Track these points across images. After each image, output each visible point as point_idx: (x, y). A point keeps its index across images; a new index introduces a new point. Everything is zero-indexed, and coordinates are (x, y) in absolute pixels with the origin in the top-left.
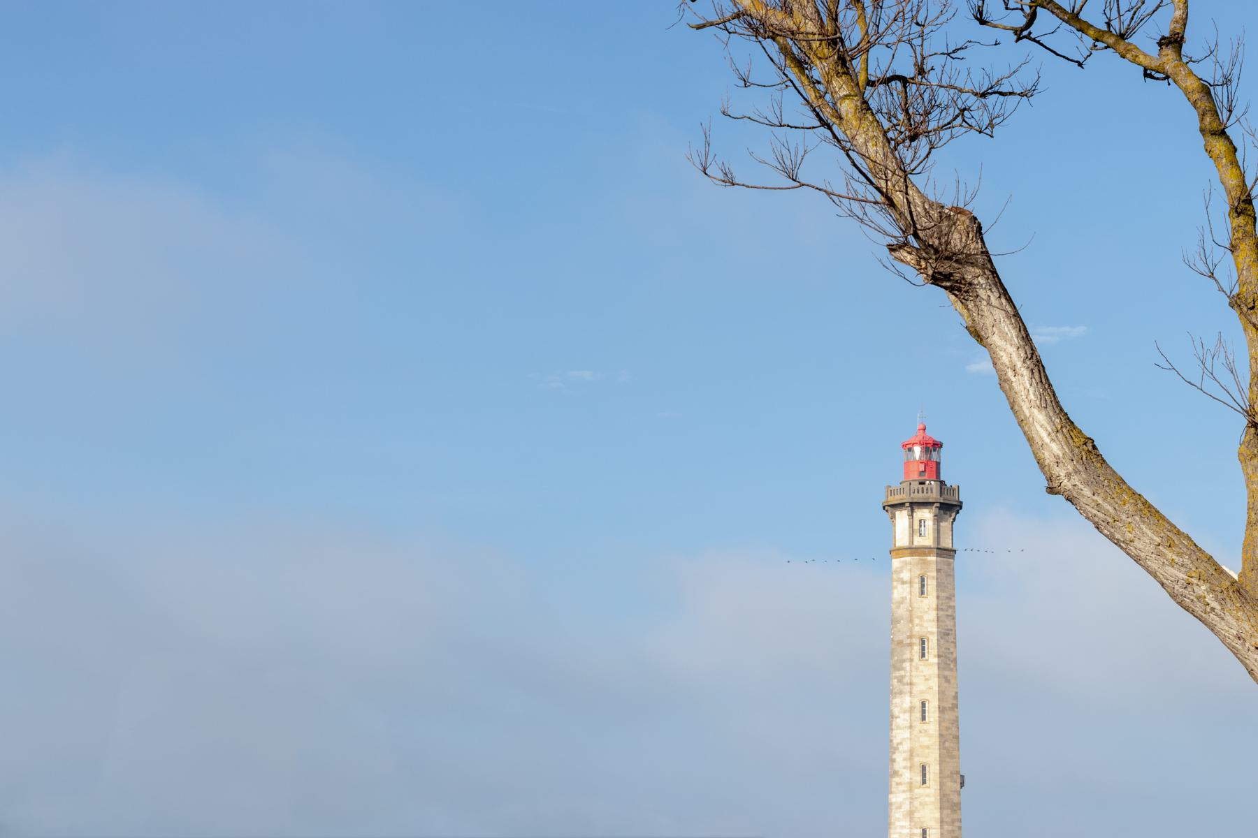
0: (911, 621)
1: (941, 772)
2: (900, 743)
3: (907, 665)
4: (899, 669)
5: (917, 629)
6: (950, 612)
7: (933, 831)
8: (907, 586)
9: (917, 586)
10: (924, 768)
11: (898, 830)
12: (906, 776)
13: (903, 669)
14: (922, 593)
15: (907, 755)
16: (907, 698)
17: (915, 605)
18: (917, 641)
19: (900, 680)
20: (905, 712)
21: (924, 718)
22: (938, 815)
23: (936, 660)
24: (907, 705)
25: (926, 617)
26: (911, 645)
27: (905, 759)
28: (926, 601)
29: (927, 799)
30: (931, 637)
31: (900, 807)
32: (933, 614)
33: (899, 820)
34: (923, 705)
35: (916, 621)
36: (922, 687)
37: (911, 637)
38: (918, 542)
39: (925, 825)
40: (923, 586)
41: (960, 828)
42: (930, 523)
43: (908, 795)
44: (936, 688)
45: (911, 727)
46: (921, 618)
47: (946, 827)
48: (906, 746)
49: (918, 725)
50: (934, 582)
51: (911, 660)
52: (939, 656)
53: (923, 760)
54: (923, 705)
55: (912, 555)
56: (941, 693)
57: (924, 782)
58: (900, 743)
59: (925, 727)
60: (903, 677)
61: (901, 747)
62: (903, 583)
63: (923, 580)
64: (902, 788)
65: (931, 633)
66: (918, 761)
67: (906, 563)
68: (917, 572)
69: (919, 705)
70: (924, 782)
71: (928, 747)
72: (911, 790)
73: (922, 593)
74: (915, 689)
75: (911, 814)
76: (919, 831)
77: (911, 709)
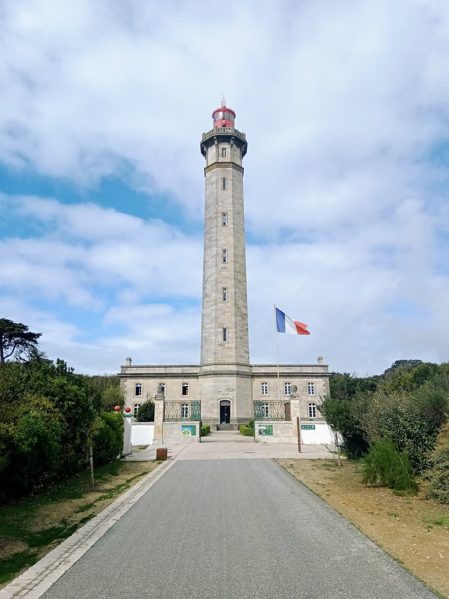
0: (217, 204)
1: (235, 293)
2: (210, 277)
3: (214, 230)
4: (209, 234)
5: (220, 208)
6: (240, 202)
7: (230, 330)
8: (214, 186)
9: (221, 184)
12: (213, 295)
13: (212, 233)
14: (224, 188)
15: (214, 283)
16: (214, 249)
17: (219, 195)
18: (220, 215)
19: (210, 240)
20: (212, 258)
22: (234, 320)
23: (232, 226)
24: (214, 253)
25: (225, 202)
26: (216, 217)
27: (212, 286)
28: (226, 192)
29: (226, 310)
30: (229, 213)
31: (209, 316)
33: (208, 324)
34: (224, 251)
35: (220, 204)
36: (223, 242)
37: (217, 213)
38: (221, 160)
39: (225, 327)
40: (224, 185)
41: (247, 329)
42: (228, 150)
43: (214, 307)
44: (232, 242)
45: (216, 265)
46: (223, 202)
47: (238, 328)
48: (213, 278)
49: (221, 265)
50: (231, 182)
51: (217, 226)
52: (234, 224)
53: (225, 286)
55: (218, 167)
56: (235, 248)
57: (225, 299)
58: (210, 277)
59: (226, 265)
60: (211, 237)
61: (210, 279)
62: (212, 184)
63: (224, 182)
64: (210, 304)
65: (230, 211)
66: (221, 286)
67: (214, 172)
68: (221, 176)
69: (221, 252)
70: (225, 299)
71: (227, 278)
72: (216, 304)
73: (224, 188)
74: (219, 243)
75: (216, 319)
76: (221, 330)
77: (217, 254)
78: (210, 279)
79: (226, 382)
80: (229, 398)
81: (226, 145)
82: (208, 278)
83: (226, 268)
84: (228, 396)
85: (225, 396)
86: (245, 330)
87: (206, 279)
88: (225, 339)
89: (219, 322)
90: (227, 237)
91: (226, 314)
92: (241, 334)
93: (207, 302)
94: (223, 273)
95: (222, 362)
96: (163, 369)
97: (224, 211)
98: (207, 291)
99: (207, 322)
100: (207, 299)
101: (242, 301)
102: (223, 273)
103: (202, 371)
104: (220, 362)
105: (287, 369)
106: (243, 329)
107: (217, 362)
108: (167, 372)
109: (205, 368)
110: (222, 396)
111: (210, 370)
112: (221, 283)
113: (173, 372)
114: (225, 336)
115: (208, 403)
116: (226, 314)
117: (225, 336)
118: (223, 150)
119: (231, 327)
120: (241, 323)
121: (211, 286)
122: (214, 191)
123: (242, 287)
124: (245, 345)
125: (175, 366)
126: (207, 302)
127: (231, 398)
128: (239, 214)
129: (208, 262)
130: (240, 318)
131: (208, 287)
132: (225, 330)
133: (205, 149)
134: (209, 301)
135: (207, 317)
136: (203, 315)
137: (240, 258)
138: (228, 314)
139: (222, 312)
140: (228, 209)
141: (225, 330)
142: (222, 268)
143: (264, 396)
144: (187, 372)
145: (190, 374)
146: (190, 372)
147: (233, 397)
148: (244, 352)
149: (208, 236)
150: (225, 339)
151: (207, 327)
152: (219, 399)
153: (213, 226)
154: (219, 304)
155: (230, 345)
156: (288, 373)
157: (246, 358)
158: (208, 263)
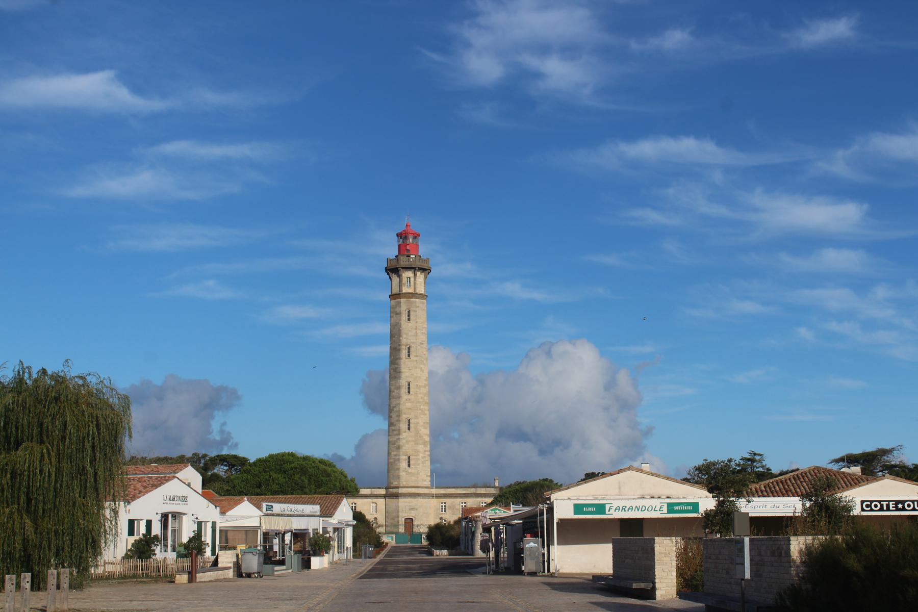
14: (409, 319)
21: (409, 392)
28: (410, 324)
32: (414, 331)
36: (407, 374)
40: (409, 316)
42: (412, 279)
46: (407, 334)
57: (409, 429)
59: (409, 397)
70: (409, 429)
73: (409, 319)
81: (410, 274)
88: (409, 466)
114: (409, 462)
117: (409, 462)
132: (409, 458)
136: (389, 442)
141: (409, 458)
149: (393, 367)
150: (409, 466)
155: (413, 471)
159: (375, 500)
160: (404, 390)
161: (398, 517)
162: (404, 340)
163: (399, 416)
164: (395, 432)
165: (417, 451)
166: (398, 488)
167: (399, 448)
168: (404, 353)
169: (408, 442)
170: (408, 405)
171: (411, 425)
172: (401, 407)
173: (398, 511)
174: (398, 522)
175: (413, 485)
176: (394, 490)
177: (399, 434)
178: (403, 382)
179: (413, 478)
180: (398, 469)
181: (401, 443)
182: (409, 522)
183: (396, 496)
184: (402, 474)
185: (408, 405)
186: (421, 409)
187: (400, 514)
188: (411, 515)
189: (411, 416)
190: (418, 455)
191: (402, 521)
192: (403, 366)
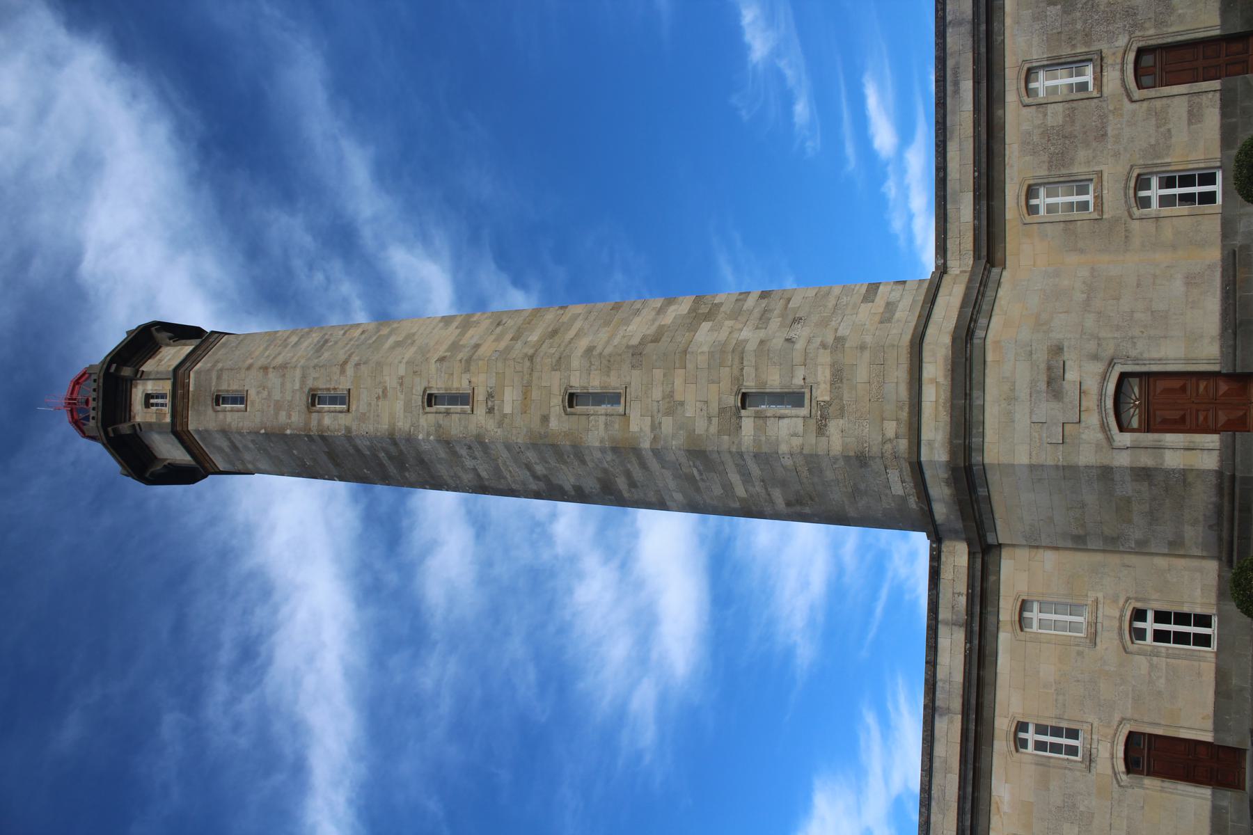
2: (528, 467)
4: (381, 465)
10: (572, 399)
11: (758, 488)
25: (277, 396)
28: (252, 394)
29: (657, 393)
30: (310, 383)
32: (273, 378)
33: (728, 487)
36: (399, 406)
39: (733, 401)
46: (278, 406)
53: (557, 402)
54: (430, 399)
57: (614, 398)
58: (528, 467)
59: (480, 396)
60: (390, 457)
70: (614, 398)
78: (540, 469)
79: (1011, 399)
80: (1104, 378)
82: (536, 477)
83: (490, 396)
84: (1092, 385)
85: (1090, 402)
86: (764, 303)
87: (542, 485)
89: (713, 429)
90: (385, 391)
91: (678, 397)
92: (775, 322)
93: (633, 484)
94: (508, 409)
95: (904, 415)
96: (940, 725)
97: (301, 400)
98: (591, 485)
99: (718, 491)
100: (621, 483)
101: (637, 320)
102: (508, 409)
103: (959, 525)
104: (903, 430)
105: (957, 91)
106: (756, 313)
107: (903, 444)
108: (957, 704)
109: (941, 511)
110: (1093, 419)
111: (947, 482)
112: (545, 419)
113: (959, 677)
115: (1128, 500)
116: (678, 397)
118: (152, 405)
119: (736, 372)
120: (729, 323)
121: (565, 463)
122: (253, 441)
123: (578, 325)
124: (831, 304)
125: (932, 663)
126: (633, 484)
127: (1099, 367)
128: (326, 341)
129: (479, 475)
130: (706, 326)
131: (572, 480)
133: (158, 468)
134: (628, 475)
135: (698, 490)
137: (471, 332)
138: (678, 382)
139: (670, 412)
140: (297, 386)
142: (490, 411)
143: (1099, 198)
144: (963, 600)
145: (971, 585)
146: (962, 587)
147: (1095, 357)
148: (865, 308)
149: (392, 470)
151: (740, 491)
152: (1109, 439)
153: (352, 451)
154: (634, 427)
156: (976, 82)
157: (895, 296)
158: (484, 474)
159: (1007, 610)
160: (458, 423)
161: (1106, 473)
162: (294, 419)
163: (556, 450)
164: (638, 474)
165: (719, 354)
166: (917, 469)
167: (698, 454)
168: (331, 420)
169: (672, 406)
170: (510, 400)
171: (595, 383)
172: (520, 439)
173: (1069, 472)
174: (1143, 474)
175: (899, 375)
176: (940, 492)
177: (636, 451)
178: (425, 425)
179: (862, 374)
180: (813, 462)
181: (677, 443)
182: (1154, 399)
183: (968, 477)
184: (837, 439)
185: (510, 400)
186: (541, 342)
187: (1087, 457)
188: (1088, 378)
189: (554, 384)
190: (739, 350)
191: (1128, 448)
192: (369, 428)
